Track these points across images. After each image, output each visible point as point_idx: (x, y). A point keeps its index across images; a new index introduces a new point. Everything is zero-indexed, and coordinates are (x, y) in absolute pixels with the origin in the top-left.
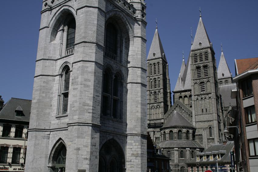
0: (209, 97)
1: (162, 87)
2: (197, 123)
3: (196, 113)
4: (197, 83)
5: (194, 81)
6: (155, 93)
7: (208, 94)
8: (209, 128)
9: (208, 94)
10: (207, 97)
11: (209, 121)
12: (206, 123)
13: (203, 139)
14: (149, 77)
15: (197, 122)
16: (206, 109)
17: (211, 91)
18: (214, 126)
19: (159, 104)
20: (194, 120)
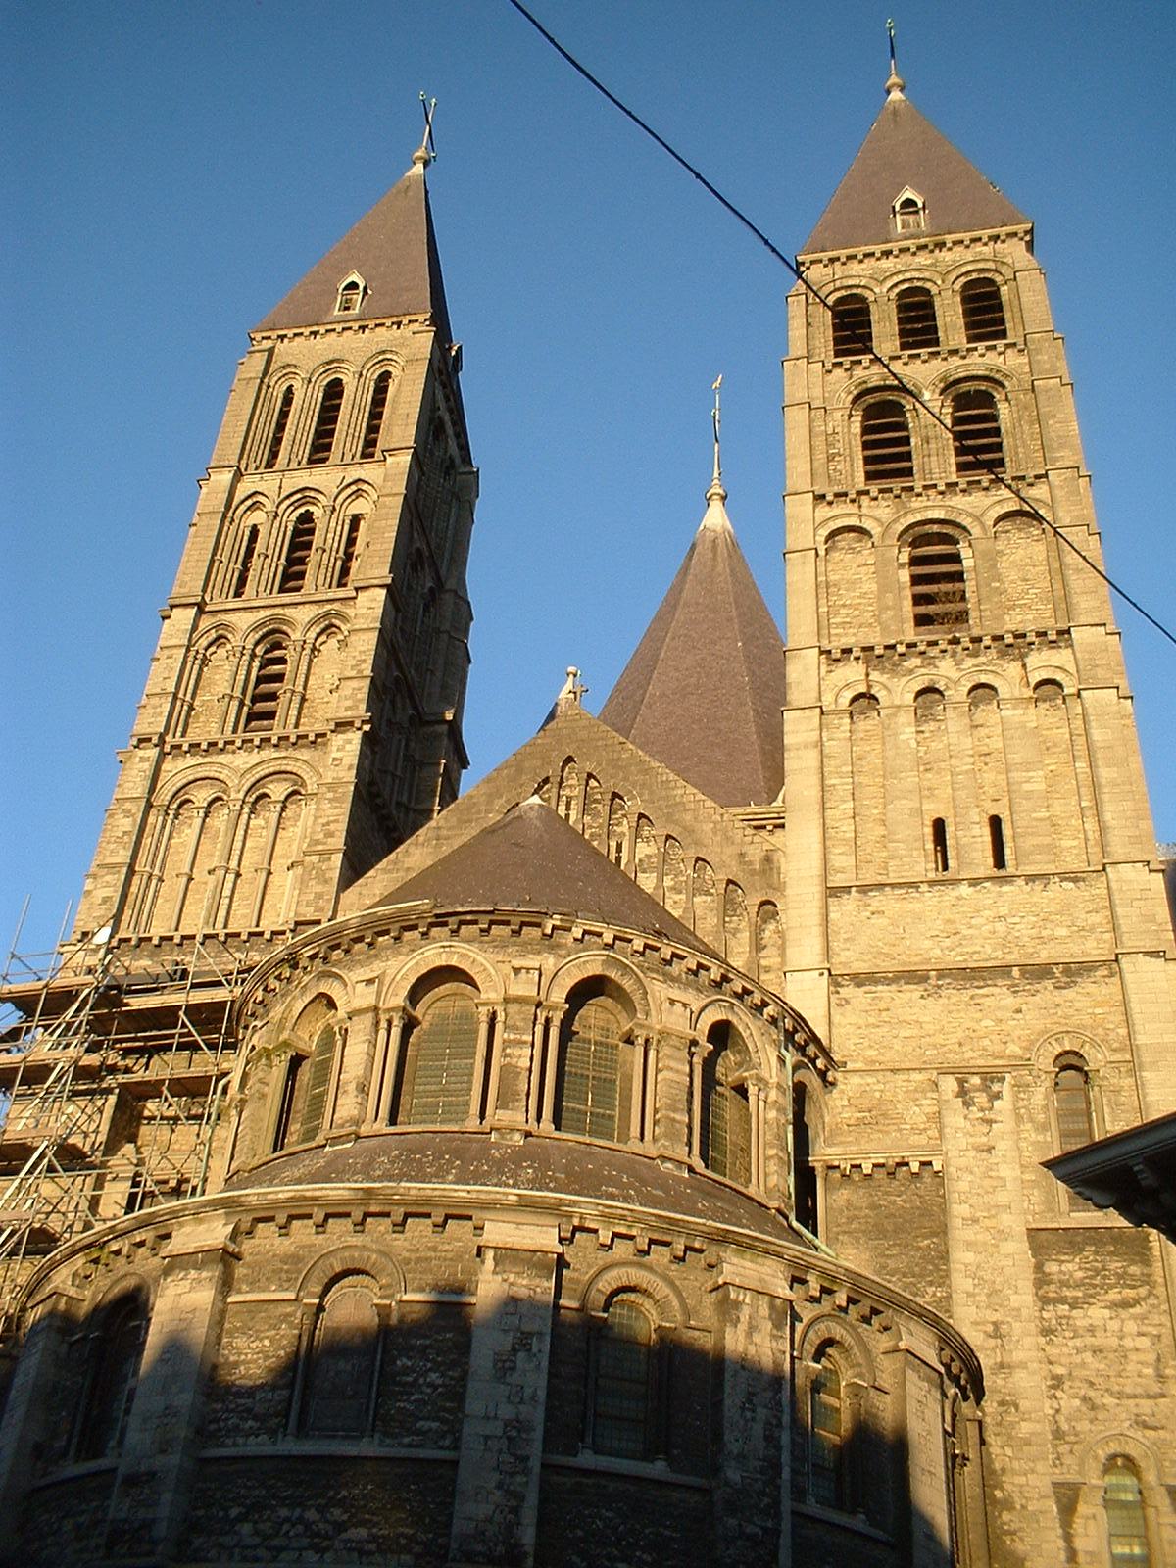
0: (1035, 678)
1: (382, 572)
2: (848, 991)
3: (842, 860)
4: (862, 532)
5: (824, 511)
6: (273, 638)
7: (1015, 645)
8: (1045, 1061)
9: (1015, 645)
10: (1008, 677)
11: (1039, 972)
12: (999, 997)
13: (960, 1233)
14: (239, 476)
15: (859, 980)
16: (995, 823)
17: (1064, 603)
18: (1141, 1039)
19: (305, 754)
20: (806, 949)
